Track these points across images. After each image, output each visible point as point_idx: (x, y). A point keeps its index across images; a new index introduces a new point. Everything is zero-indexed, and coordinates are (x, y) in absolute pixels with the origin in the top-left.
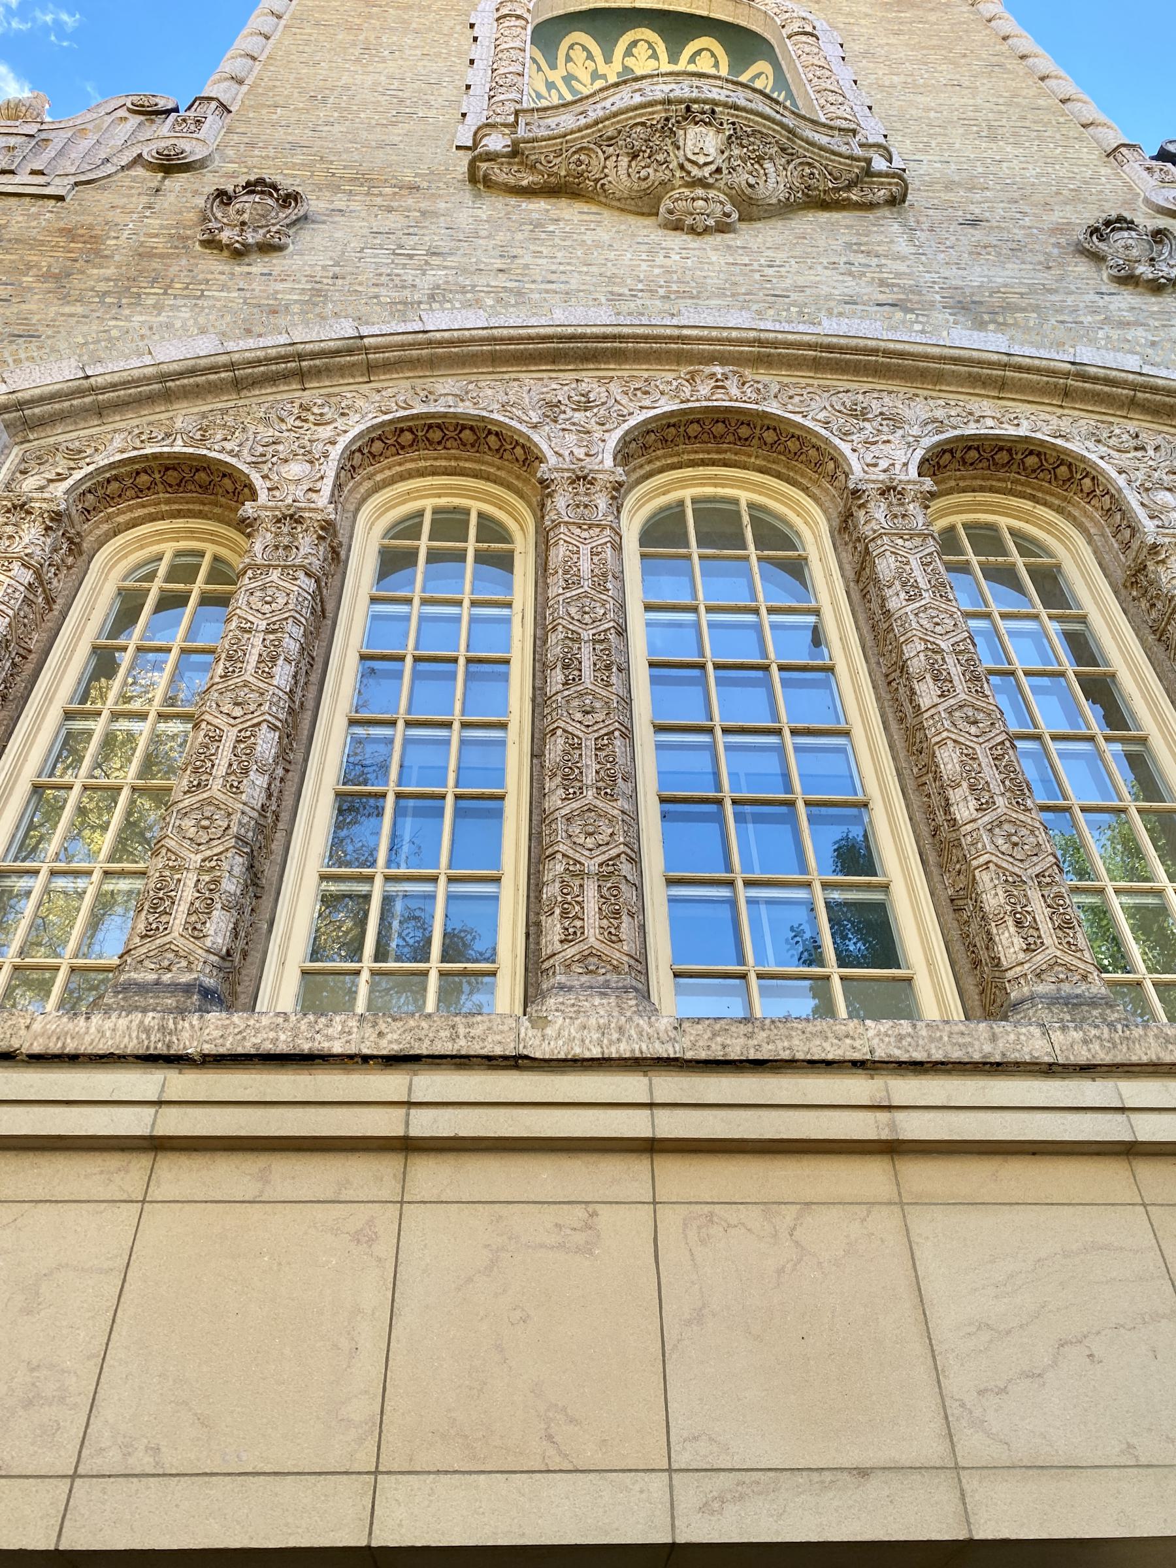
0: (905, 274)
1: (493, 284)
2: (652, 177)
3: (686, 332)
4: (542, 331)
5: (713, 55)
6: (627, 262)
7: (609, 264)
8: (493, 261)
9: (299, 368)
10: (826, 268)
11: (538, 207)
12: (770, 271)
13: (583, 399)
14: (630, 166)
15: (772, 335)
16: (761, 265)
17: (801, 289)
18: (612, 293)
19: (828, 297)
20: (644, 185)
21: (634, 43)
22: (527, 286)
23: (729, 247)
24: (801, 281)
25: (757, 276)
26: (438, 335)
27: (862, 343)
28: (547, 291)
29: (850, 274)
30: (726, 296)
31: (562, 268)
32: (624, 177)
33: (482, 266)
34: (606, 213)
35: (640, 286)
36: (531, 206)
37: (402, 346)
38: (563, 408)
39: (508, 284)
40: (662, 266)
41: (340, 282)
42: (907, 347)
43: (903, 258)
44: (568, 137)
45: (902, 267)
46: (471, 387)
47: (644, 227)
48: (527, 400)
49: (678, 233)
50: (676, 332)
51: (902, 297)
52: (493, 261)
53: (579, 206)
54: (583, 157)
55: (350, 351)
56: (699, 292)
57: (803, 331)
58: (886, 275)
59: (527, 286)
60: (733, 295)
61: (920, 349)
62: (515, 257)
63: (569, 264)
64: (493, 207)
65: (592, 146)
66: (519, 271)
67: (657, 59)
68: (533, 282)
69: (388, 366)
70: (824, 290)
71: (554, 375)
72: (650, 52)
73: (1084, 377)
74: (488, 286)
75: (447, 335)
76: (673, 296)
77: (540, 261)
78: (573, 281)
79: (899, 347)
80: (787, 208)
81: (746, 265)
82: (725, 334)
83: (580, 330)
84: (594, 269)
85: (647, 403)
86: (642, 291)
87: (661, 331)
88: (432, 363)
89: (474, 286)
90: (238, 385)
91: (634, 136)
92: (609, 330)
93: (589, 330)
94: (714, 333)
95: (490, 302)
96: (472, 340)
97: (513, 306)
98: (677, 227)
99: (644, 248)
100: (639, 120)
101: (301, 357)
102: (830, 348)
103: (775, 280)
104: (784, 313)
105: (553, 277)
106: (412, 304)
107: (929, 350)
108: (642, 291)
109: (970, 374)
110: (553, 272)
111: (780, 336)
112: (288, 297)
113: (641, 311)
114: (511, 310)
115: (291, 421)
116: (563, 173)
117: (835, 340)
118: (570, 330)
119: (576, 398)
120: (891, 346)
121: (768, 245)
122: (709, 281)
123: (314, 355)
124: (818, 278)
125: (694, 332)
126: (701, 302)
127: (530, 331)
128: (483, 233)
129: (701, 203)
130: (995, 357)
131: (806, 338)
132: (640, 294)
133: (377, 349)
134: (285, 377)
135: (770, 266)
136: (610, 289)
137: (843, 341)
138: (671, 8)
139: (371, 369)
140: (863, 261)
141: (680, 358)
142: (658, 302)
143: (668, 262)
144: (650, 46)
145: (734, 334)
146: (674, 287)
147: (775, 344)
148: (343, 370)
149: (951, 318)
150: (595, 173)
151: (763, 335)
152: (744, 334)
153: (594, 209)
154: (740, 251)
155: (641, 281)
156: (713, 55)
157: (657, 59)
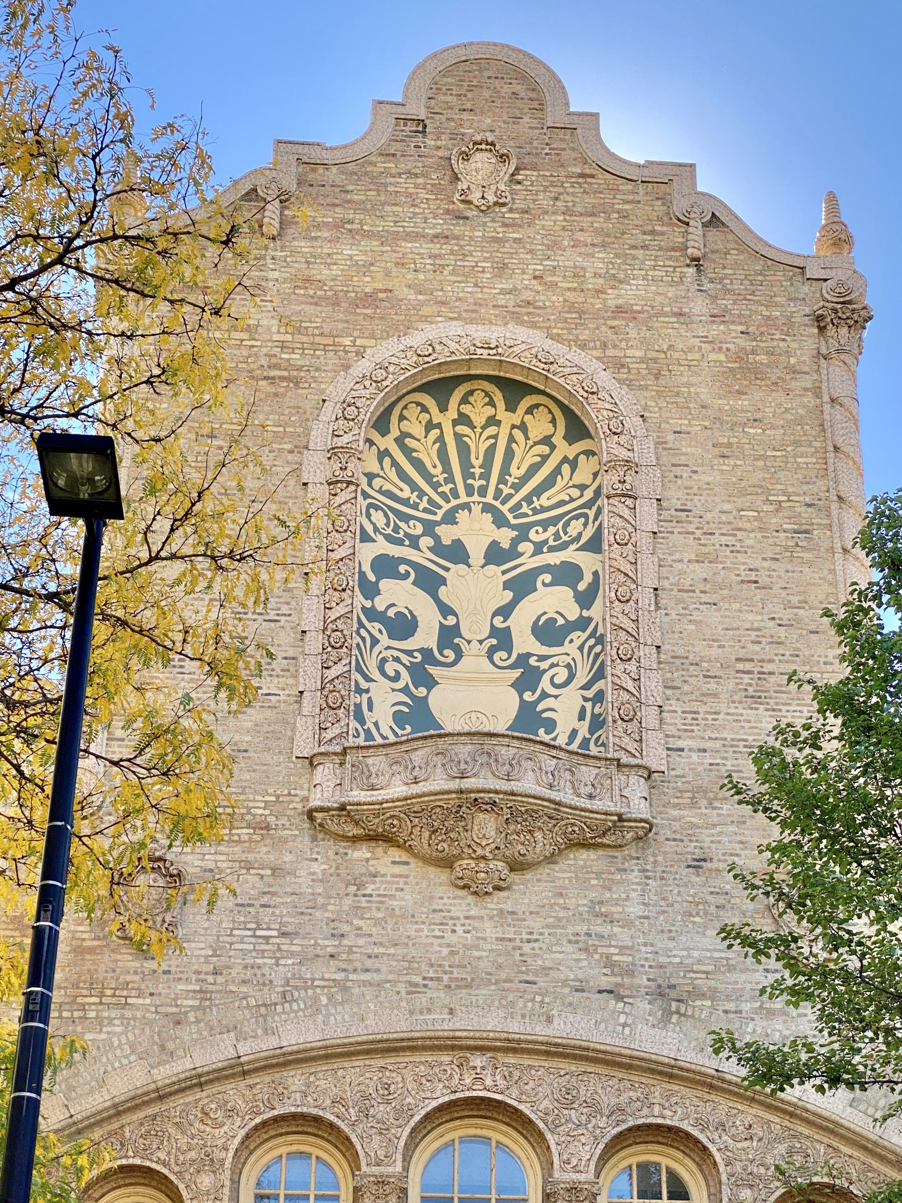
0: (626, 947)
1: (327, 976)
2: (447, 851)
3: (458, 1034)
4: (359, 1039)
5: (550, 412)
6: (425, 941)
7: (410, 943)
8: (327, 943)
9: (199, 1081)
10: (570, 941)
11: (361, 853)
12: (527, 948)
13: (386, 1092)
14: (430, 838)
15: (517, 1036)
16: (522, 941)
17: (546, 970)
18: (411, 984)
19: (565, 982)
20: (440, 855)
21: (471, 393)
22: (351, 977)
23: (501, 911)
24: (549, 959)
25: (517, 957)
26: (289, 1049)
27: (578, 1043)
28: (365, 983)
29: (586, 950)
30: (491, 984)
31: (376, 951)
32: (426, 846)
33: (318, 952)
34: (412, 860)
35: (431, 974)
36: (357, 854)
37: (266, 1058)
38: (373, 1102)
39: (339, 976)
40: (449, 945)
41: (220, 979)
42: (608, 1048)
43: (627, 924)
44: (385, 805)
45: (624, 936)
46: (312, 1079)
47: (441, 884)
48: (349, 1094)
49: (464, 893)
50: (451, 1034)
51: (618, 979)
52: (327, 943)
53: (396, 854)
54: (395, 822)
55: (231, 1067)
56: (473, 979)
57: (540, 1031)
58: (612, 950)
59: (351, 977)
60: (496, 983)
61: (617, 1050)
62: (342, 935)
63: (381, 944)
64: (329, 847)
65: (402, 815)
66: (344, 957)
67: (494, 406)
68: (355, 970)
69: (256, 1070)
70: (565, 973)
71: (367, 1062)
72: (487, 399)
73: (723, 1080)
74: (323, 979)
75: (295, 1048)
76: (453, 985)
77: (361, 941)
78: (384, 969)
79: (603, 1048)
80: (551, 859)
81: (510, 940)
82: (485, 1035)
83: (385, 1037)
84: (400, 951)
85: (429, 1095)
86: (432, 979)
87: (441, 1034)
88: (285, 1064)
89: (313, 980)
90: (161, 1098)
91: (434, 817)
92: (405, 1035)
93: (391, 1036)
94: (478, 1035)
95: (324, 1000)
96: (312, 1049)
97: (341, 1004)
98: (466, 887)
99: (438, 917)
100: (438, 803)
101: (200, 1076)
102: (557, 1045)
103: (529, 960)
104: (530, 1004)
105: (369, 963)
106: (270, 1005)
107: (623, 1051)
108: (432, 979)
109: (649, 1069)
110: (370, 957)
111: (522, 1037)
112: (186, 1002)
113: (430, 1006)
114: (339, 1008)
115: (196, 1125)
116: (381, 830)
117: (560, 1041)
118: (379, 1037)
119: (381, 1092)
120: (598, 1047)
121: (532, 909)
122: (482, 964)
123: (208, 1073)
124: (561, 956)
125: (465, 1034)
126: (472, 992)
127: (351, 1040)
128: (320, 900)
129: (482, 875)
130: (666, 1060)
131: (541, 1039)
132: (430, 983)
133: (249, 1062)
134: (190, 1087)
135: (529, 941)
136: (408, 978)
137: (564, 1041)
138: (508, 375)
139: (244, 1073)
140: (599, 929)
141: (453, 1048)
142: (442, 994)
143: (453, 938)
144: (487, 394)
145: (491, 1035)
146: (455, 975)
147: (519, 1041)
148: (226, 1077)
149: (648, 1007)
150: (404, 835)
151: (511, 1036)
152: (497, 1035)
153: (404, 857)
154: (509, 917)
155: (432, 966)
156: (550, 412)
157: (494, 406)
